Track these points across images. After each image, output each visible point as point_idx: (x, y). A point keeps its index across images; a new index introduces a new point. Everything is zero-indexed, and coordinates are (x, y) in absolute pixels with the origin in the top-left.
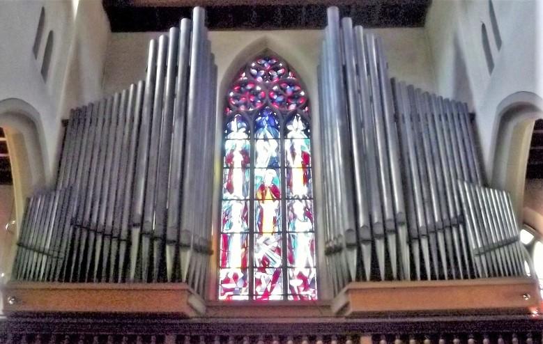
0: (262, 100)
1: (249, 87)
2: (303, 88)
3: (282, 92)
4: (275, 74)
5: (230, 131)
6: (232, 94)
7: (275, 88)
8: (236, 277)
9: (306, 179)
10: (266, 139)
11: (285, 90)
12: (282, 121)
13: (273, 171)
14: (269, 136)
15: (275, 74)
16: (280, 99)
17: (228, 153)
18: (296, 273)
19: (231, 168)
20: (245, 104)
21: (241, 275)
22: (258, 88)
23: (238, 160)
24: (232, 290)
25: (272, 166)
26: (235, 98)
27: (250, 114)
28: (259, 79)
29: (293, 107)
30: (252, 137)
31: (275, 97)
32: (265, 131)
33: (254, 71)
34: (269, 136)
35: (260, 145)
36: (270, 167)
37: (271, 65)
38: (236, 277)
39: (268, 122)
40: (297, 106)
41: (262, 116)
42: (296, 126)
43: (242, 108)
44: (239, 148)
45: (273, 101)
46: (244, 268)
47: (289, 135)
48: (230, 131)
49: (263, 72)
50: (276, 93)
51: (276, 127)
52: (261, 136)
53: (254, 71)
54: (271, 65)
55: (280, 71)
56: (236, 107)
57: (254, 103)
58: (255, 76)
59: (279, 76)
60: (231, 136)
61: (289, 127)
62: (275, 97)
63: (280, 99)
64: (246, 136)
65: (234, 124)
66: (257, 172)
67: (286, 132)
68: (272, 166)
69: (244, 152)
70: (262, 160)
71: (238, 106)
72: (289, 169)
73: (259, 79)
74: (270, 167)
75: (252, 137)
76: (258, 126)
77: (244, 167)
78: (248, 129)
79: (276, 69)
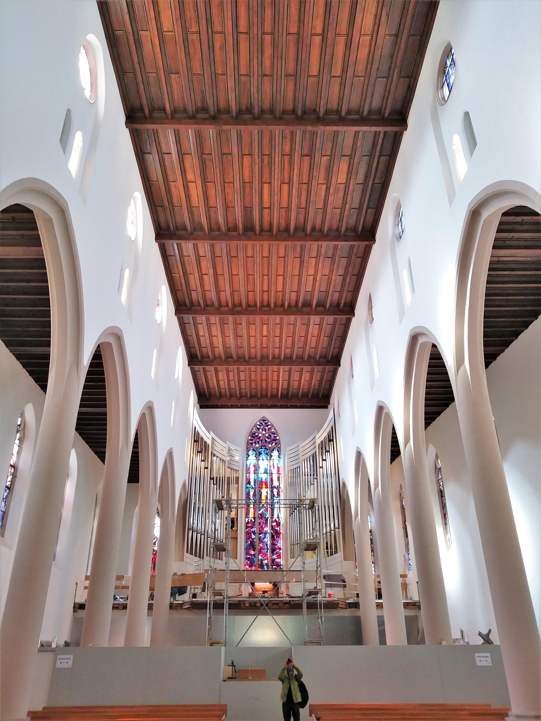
0: (262, 441)
1: (256, 434)
2: (278, 436)
3: (269, 437)
4: (267, 428)
5: (249, 456)
6: (249, 438)
7: (267, 435)
8: (251, 520)
9: (279, 479)
10: (263, 460)
11: (271, 436)
12: (270, 453)
13: (266, 475)
14: (264, 458)
15: (267, 428)
16: (269, 440)
17: (248, 466)
18: (274, 520)
19: (250, 473)
20: (255, 443)
21: (253, 520)
22: (260, 435)
23: (252, 469)
24: (249, 527)
25: (266, 472)
26: (251, 440)
27: (257, 448)
28: (261, 430)
29: (274, 444)
30: (258, 460)
31: (267, 439)
32: (263, 456)
33: (258, 427)
34: (264, 458)
35: (261, 462)
36: (265, 473)
37: (266, 423)
38: (251, 520)
39: (264, 451)
40: (276, 443)
41: (262, 448)
42: (275, 453)
43: (254, 444)
44: (252, 464)
45: (266, 441)
46: (254, 518)
47: (272, 458)
48: (249, 456)
49: (262, 427)
50: (267, 437)
51: (267, 454)
52: (261, 458)
53: (258, 427)
54: (266, 423)
55: (269, 427)
56: (250, 445)
57: (258, 442)
58: (259, 429)
59: (269, 429)
60: (250, 458)
61: (272, 454)
62: (267, 439)
63: (269, 440)
64: (255, 458)
65: (251, 452)
66: (260, 476)
67: (271, 456)
68: (266, 472)
69: (254, 466)
70: (261, 470)
71: (252, 444)
72: (272, 473)
73: (261, 430)
74: (265, 473)
75: (258, 460)
76: (260, 454)
77: (255, 473)
78: (256, 455)
79: (267, 426)
